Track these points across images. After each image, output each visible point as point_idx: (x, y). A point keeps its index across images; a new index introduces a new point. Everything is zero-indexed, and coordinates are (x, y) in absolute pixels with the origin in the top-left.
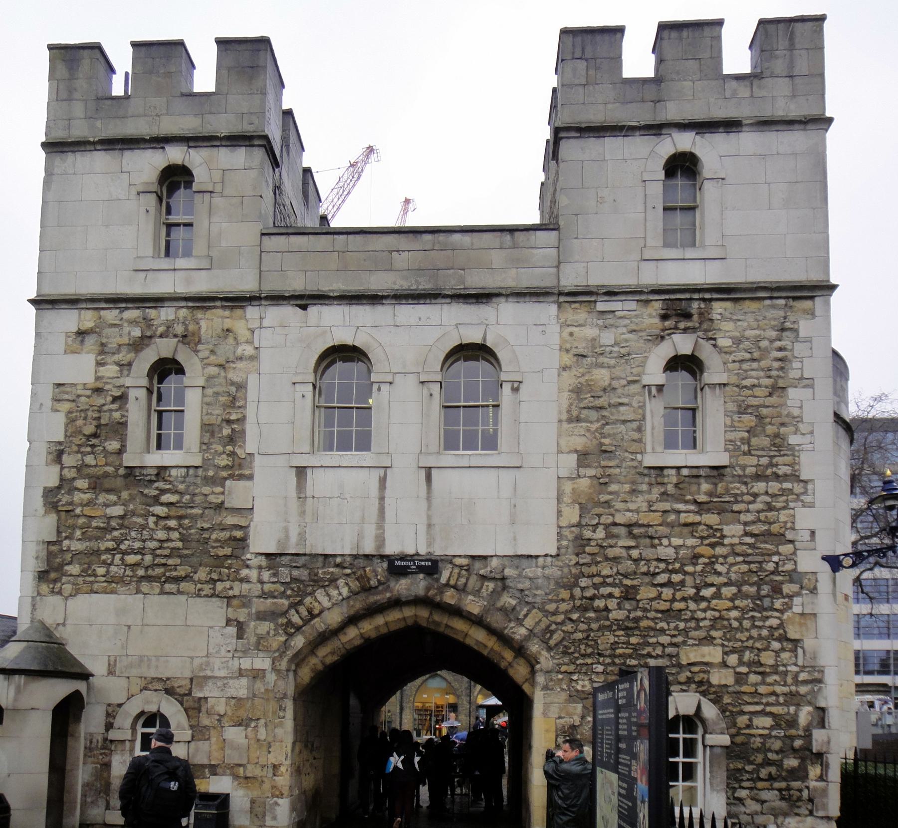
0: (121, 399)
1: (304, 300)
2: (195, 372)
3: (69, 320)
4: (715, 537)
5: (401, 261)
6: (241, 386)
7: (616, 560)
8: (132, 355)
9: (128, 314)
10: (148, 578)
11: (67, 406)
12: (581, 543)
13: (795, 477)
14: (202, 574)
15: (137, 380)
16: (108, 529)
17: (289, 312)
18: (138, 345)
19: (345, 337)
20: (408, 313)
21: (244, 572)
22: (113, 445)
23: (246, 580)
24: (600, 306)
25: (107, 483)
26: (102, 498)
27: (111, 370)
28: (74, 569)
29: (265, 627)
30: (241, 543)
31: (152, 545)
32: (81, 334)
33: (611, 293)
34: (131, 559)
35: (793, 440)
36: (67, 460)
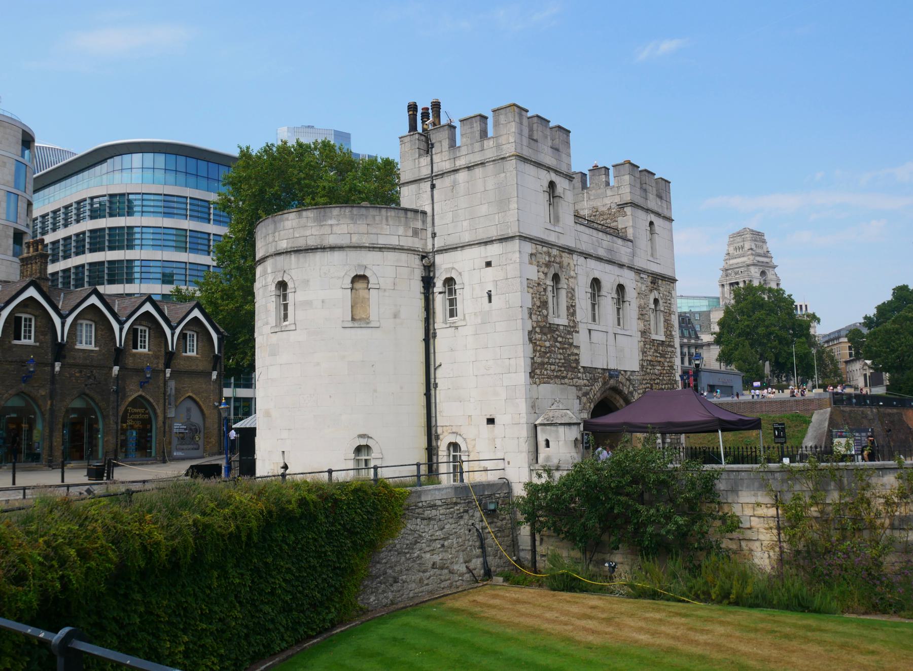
0: (545, 290)
1: (587, 256)
2: (563, 283)
3: (529, 248)
4: (663, 366)
5: (605, 244)
6: (573, 290)
7: (648, 374)
8: (546, 270)
9: (545, 249)
10: (557, 377)
11: (531, 290)
12: (642, 366)
13: (673, 346)
14: (570, 373)
15: (549, 282)
16: (546, 353)
17: (581, 260)
18: (548, 265)
19: (597, 275)
20: (609, 267)
21: (580, 375)
22: (545, 312)
23: (579, 378)
24: (642, 276)
25: (546, 330)
26: (544, 337)
27: (542, 276)
28: (538, 371)
29: (584, 399)
30: (577, 361)
31: (557, 361)
32: (531, 255)
33: (645, 272)
34: (553, 367)
35: (673, 333)
36: (534, 317)
